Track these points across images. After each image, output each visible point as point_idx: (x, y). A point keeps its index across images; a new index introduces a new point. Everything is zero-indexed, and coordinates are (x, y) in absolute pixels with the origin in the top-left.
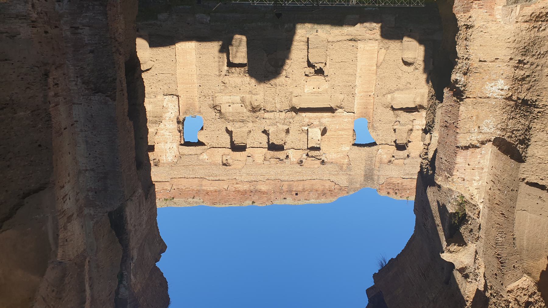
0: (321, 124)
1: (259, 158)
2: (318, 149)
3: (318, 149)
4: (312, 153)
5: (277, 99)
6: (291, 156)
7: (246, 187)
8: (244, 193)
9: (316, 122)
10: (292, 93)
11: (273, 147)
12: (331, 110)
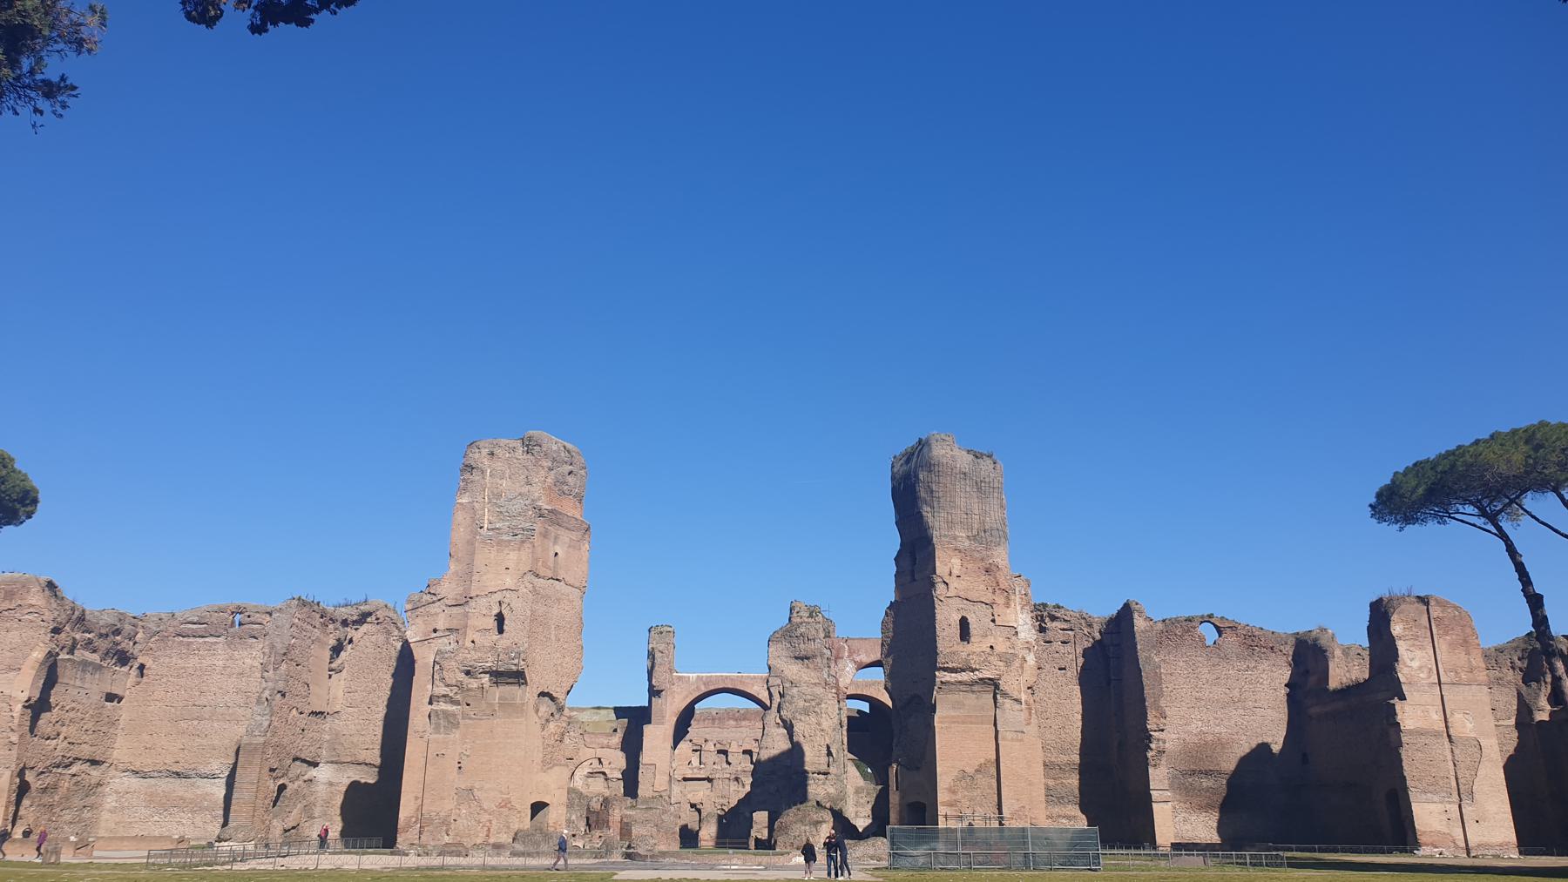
0: (692, 769)
1: (734, 743)
2: (693, 750)
3: (693, 750)
4: (699, 748)
5: (721, 787)
6: (713, 746)
7: (743, 723)
8: (744, 719)
9: (695, 770)
10: (712, 791)
11: (725, 752)
12: (685, 779)
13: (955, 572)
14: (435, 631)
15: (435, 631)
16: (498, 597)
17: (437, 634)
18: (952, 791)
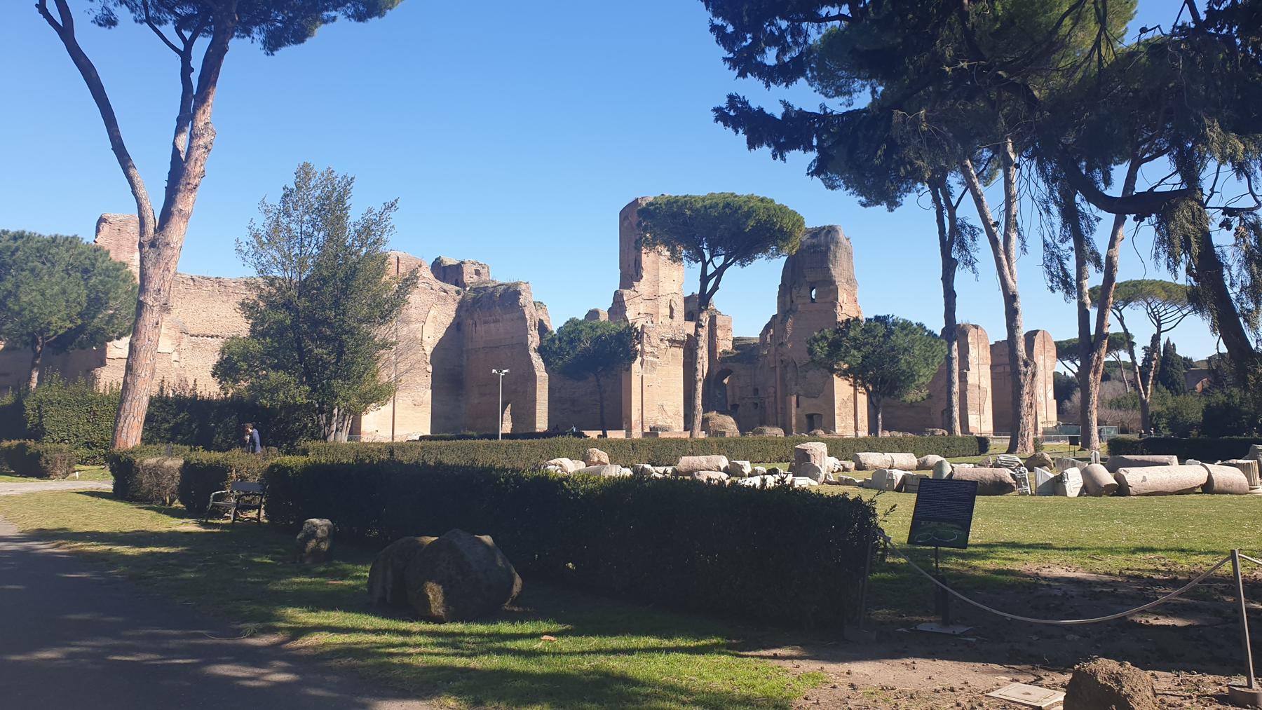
13: (845, 301)
14: (639, 314)
15: (639, 314)
16: (670, 297)
17: (641, 316)
18: (840, 409)
